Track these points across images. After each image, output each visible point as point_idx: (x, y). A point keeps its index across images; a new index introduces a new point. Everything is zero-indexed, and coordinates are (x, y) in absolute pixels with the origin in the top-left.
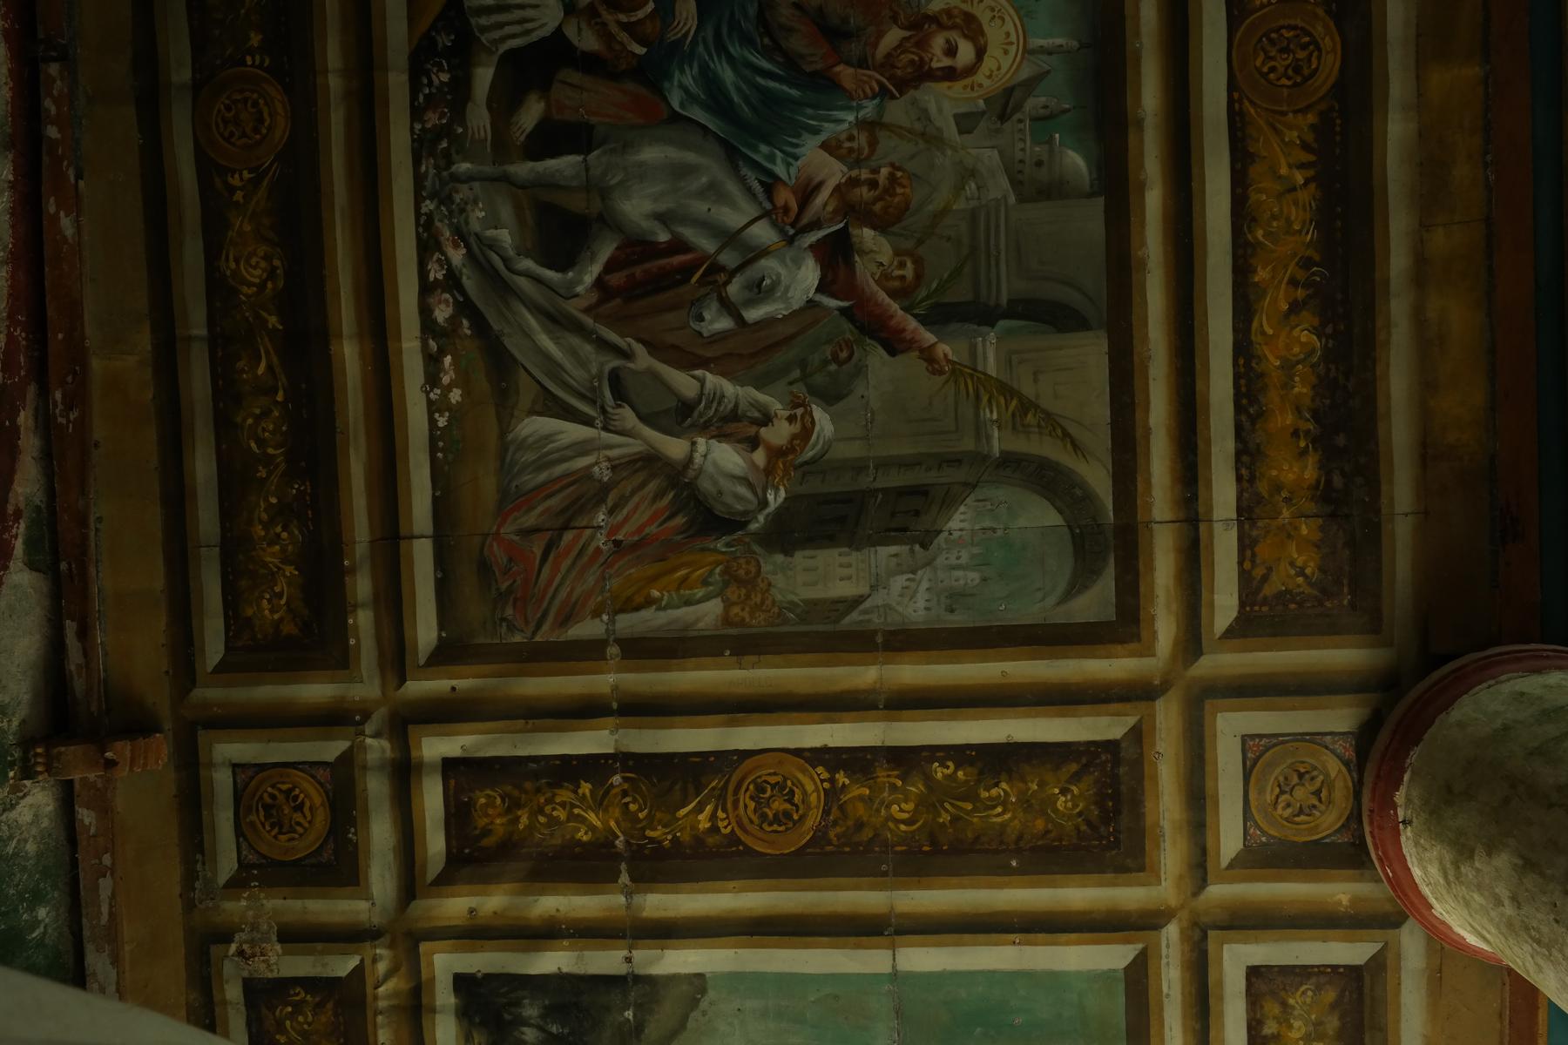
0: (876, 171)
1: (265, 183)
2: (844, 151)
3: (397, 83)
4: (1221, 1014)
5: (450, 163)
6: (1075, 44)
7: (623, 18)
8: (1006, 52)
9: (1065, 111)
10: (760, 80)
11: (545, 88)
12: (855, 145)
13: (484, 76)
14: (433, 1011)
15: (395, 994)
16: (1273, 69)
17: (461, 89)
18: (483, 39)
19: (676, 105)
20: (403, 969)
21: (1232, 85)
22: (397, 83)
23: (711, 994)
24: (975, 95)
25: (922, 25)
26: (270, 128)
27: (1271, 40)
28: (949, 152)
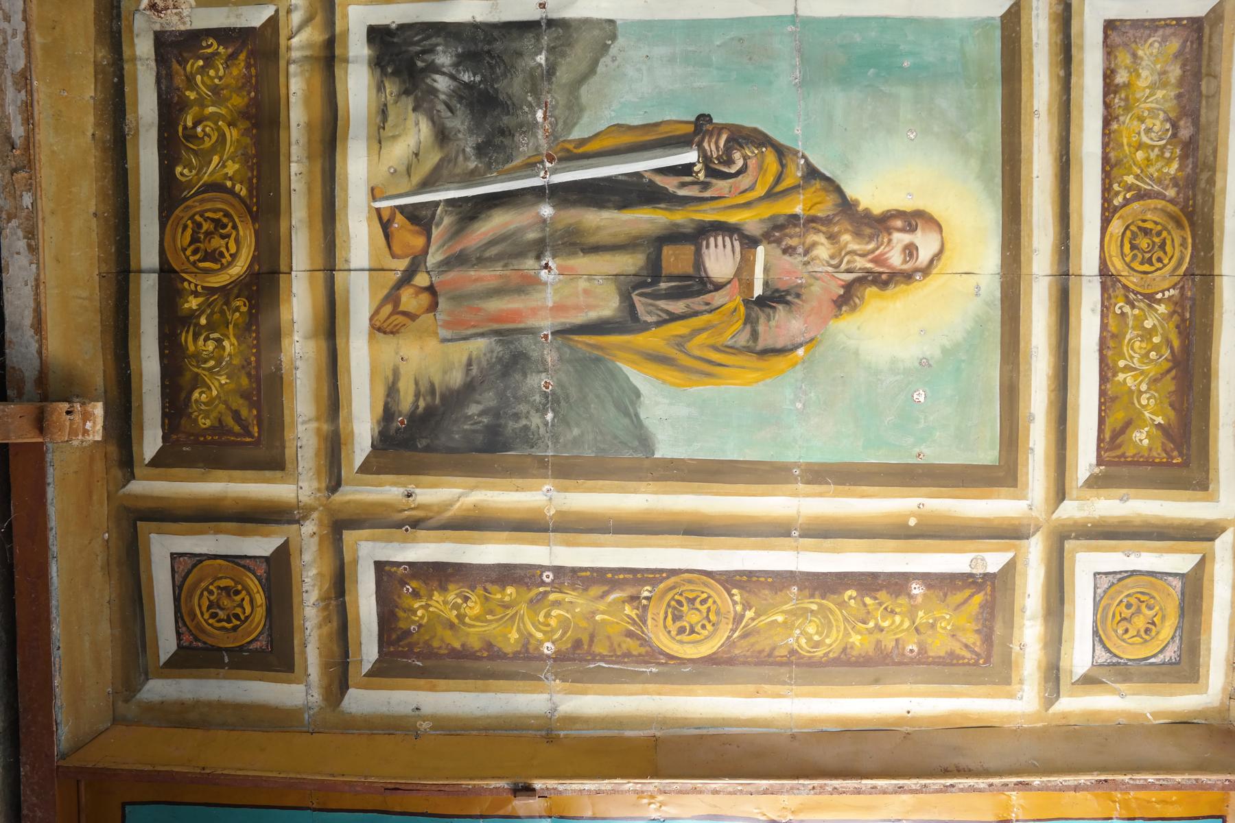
4: (1081, 62)
14: (346, 60)
15: (310, 45)
20: (319, 19)
23: (621, 41)
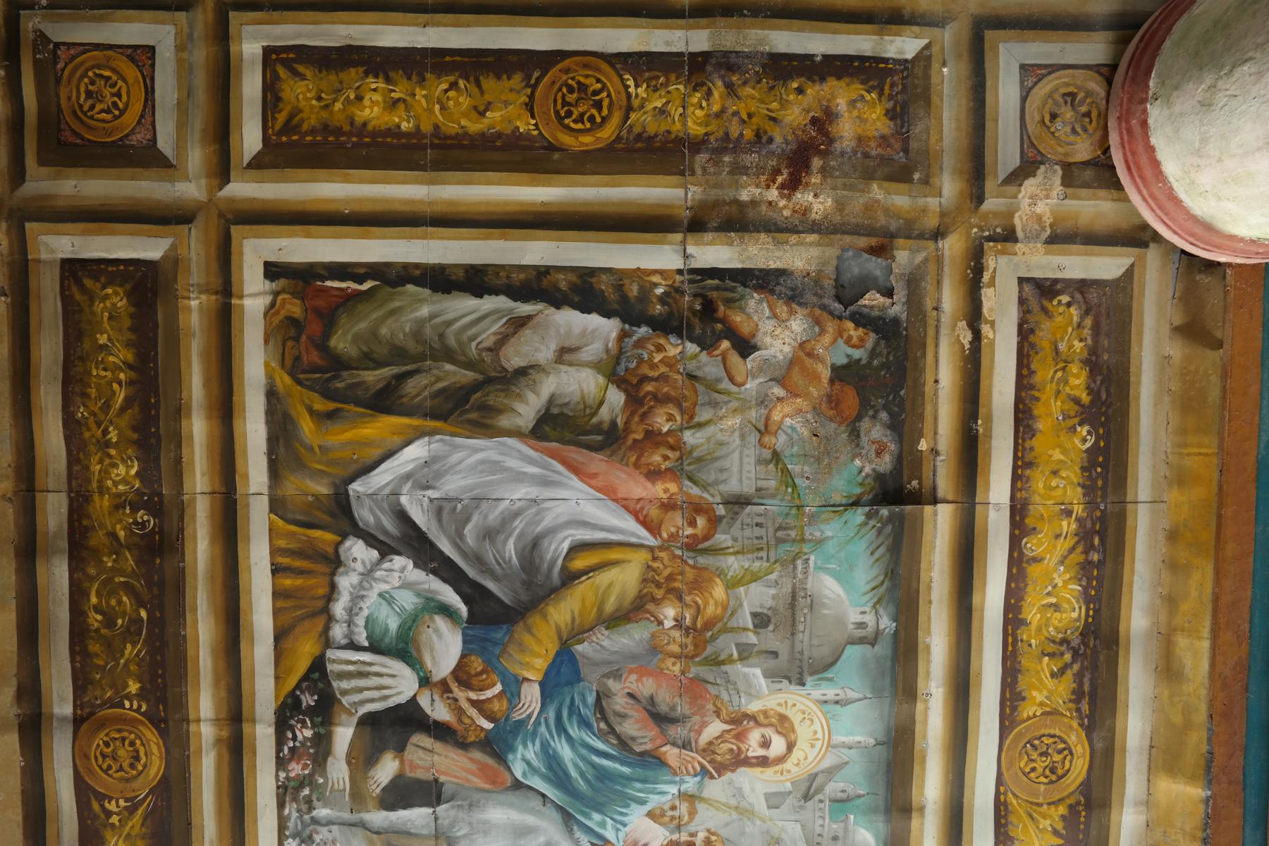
0: (693, 835)
1: (140, 811)
2: (667, 819)
3: (263, 734)
5: (311, 808)
6: (872, 741)
7: (473, 695)
8: (813, 746)
9: (860, 796)
10: (596, 759)
11: (400, 749)
12: (676, 813)
13: (343, 735)
16: (1033, 770)
17: (322, 744)
18: (344, 702)
19: (519, 775)
21: (999, 781)
22: (263, 734)
24: (783, 778)
25: (740, 722)
26: (145, 766)
27: (1035, 747)
28: (758, 822)
